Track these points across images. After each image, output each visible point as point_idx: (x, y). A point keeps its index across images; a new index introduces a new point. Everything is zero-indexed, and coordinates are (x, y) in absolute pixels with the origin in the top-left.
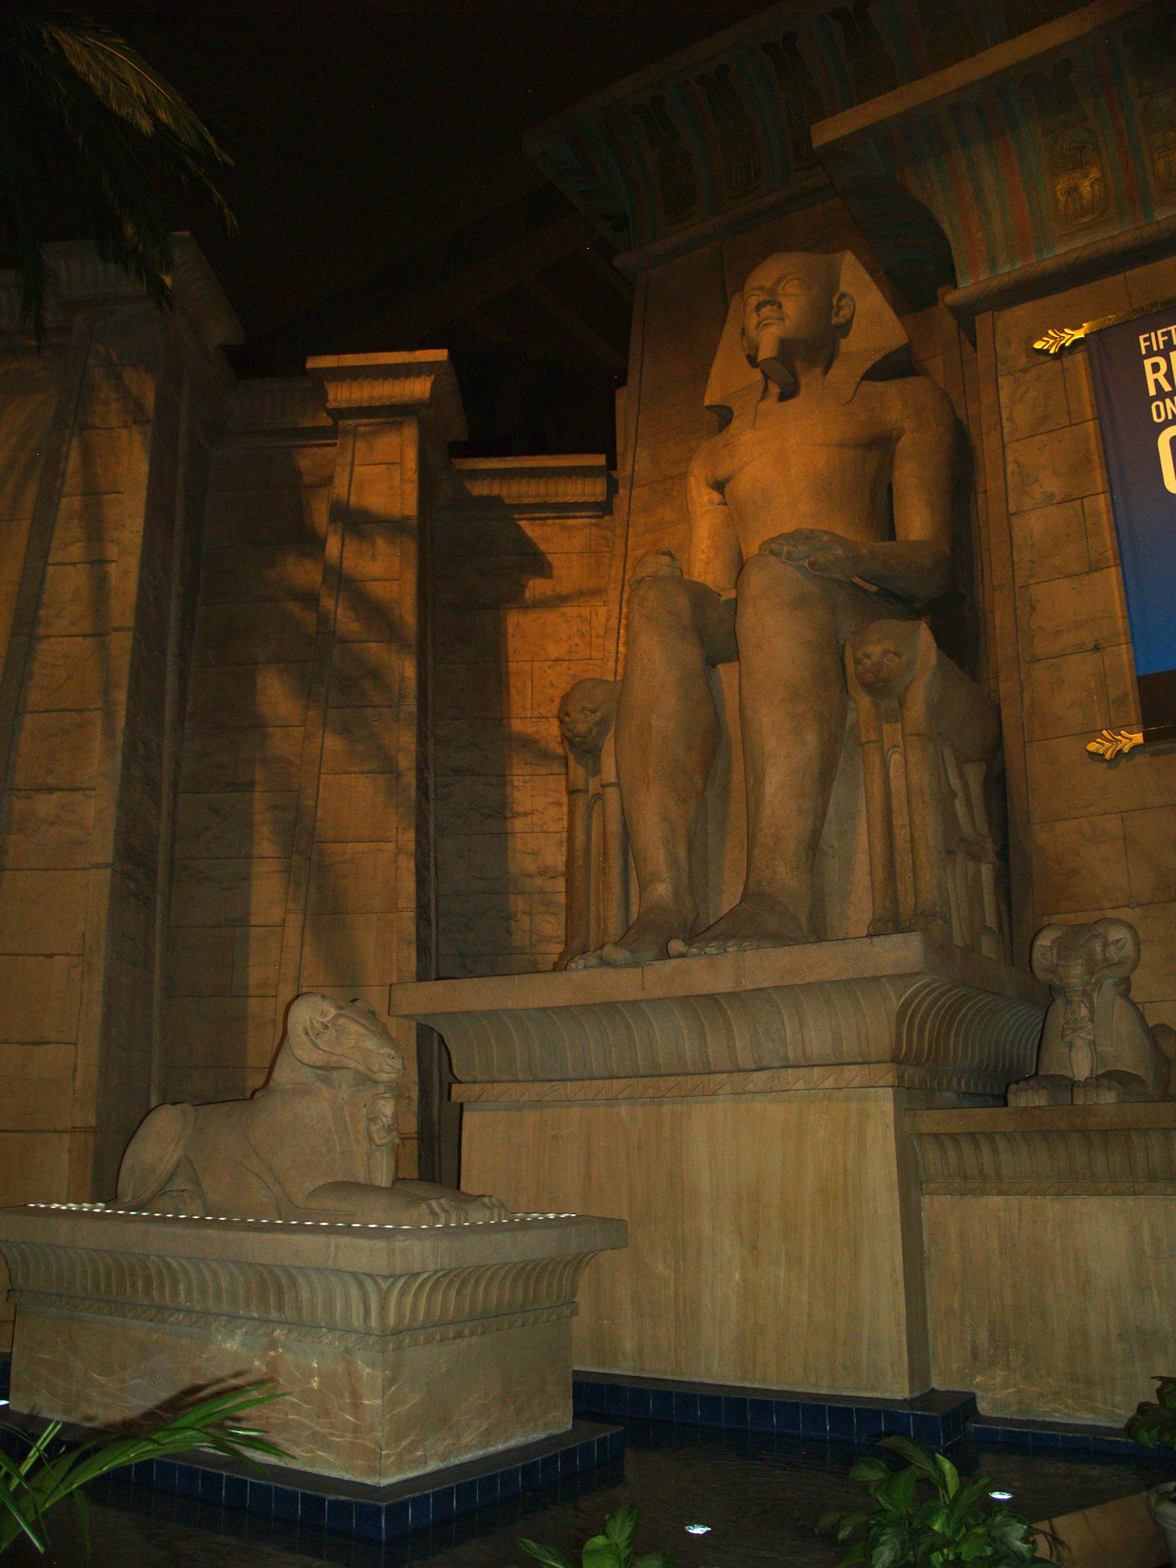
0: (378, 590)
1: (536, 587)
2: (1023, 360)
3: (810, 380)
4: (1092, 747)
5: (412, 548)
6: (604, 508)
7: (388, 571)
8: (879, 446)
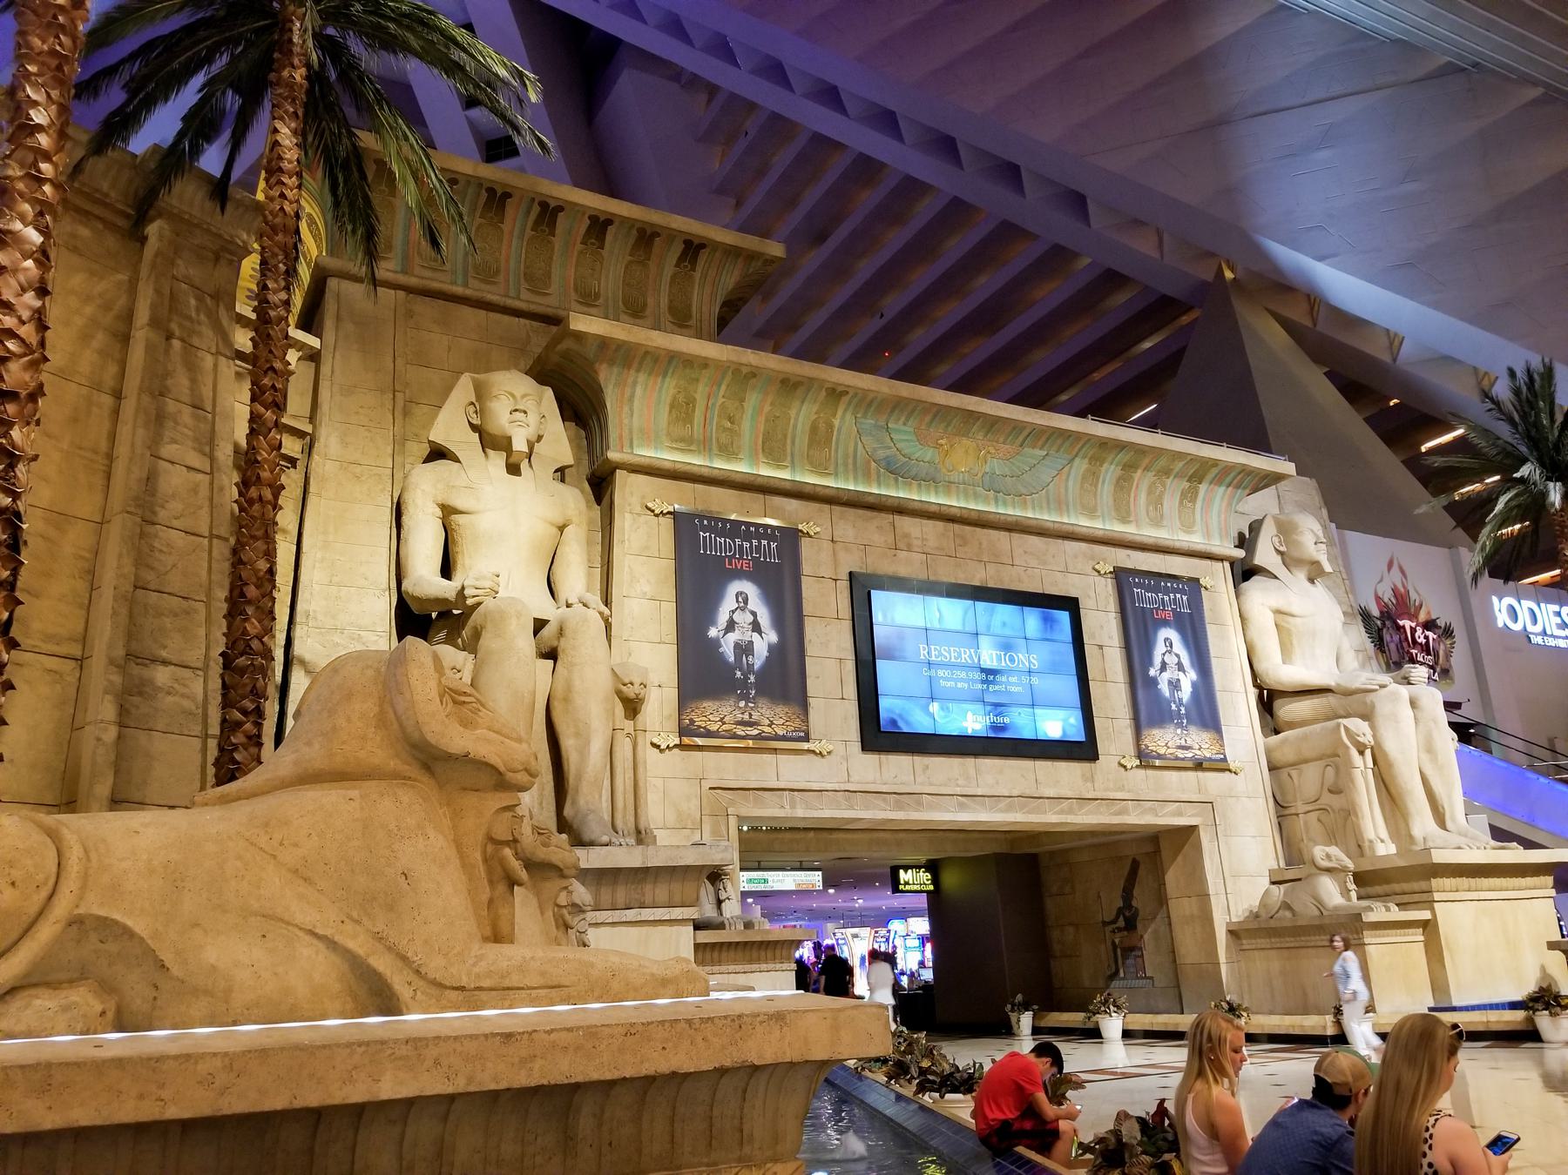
2: (638, 509)
3: (524, 465)
4: (655, 741)
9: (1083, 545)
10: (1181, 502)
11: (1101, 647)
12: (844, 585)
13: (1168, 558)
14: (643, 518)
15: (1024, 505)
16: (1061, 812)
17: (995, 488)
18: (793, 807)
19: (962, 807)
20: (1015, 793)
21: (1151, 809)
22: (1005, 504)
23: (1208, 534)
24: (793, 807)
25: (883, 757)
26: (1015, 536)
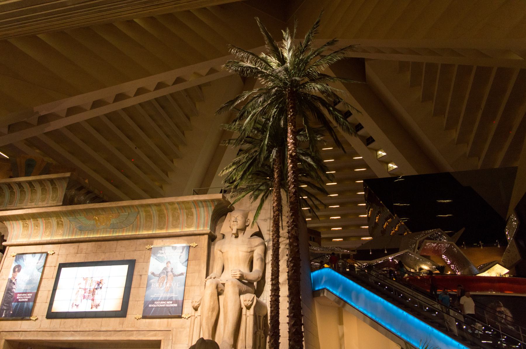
9: (144, 240)
10: (187, 217)
11: (141, 275)
15: (123, 232)
16: (107, 336)
17: (114, 228)
19: (72, 335)
20: (91, 330)
22: (116, 232)
23: (198, 226)
24: (25, 336)
25: (52, 320)
26: (119, 242)
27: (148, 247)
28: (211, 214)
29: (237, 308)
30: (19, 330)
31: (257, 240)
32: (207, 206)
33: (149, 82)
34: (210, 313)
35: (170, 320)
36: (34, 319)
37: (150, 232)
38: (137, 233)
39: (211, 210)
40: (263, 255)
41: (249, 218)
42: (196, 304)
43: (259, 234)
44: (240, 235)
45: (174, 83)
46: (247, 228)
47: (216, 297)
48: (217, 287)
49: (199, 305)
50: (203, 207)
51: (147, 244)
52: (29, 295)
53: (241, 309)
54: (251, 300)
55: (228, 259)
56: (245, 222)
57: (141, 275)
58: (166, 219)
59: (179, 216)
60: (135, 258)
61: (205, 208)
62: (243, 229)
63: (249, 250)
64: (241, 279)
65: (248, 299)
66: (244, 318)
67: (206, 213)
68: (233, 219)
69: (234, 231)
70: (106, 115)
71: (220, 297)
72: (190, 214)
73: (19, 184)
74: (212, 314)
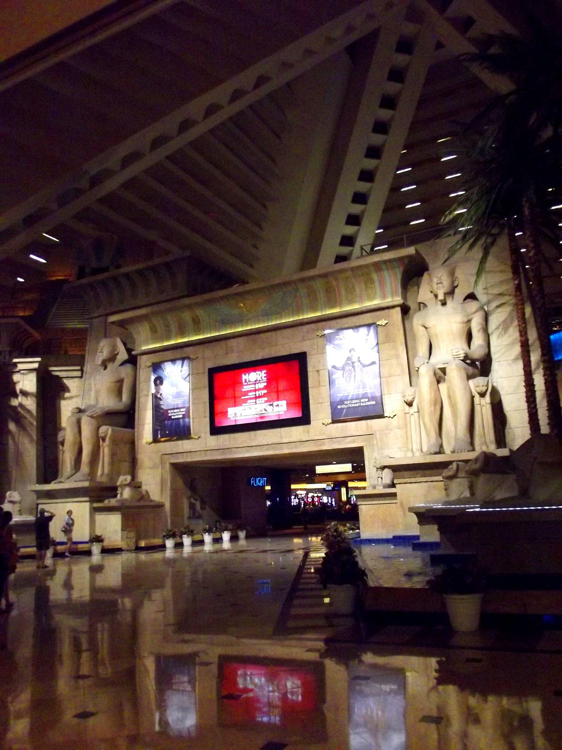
0: (29, 407)
1: (67, 395)
3: (110, 366)
5: (34, 399)
6: (81, 377)
7: (30, 404)
8: (120, 382)
9: (313, 326)
12: (207, 374)
13: (361, 316)
14: (145, 370)
17: (267, 315)
18: (187, 457)
19: (248, 451)
21: (337, 441)
27: (320, 333)
28: (399, 277)
29: (469, 397)
30: (183, 451)
31: (473, 306)
32: (392, 268)
33: (219, 94)
34: (433, 408)
35: (369, 421)
36: (196, 437)
37: (318, 314)
38: (301, 318)
39: (398, 273)
40: (484, 323)
41: (456, 275)
42: (409, 399)
43: (472, 297)
44: (449, 302)
45: (257, 86)
46: (457, 290)
47: (436, 387)
48: (435, 374)
49: (414, 398)
50: (388, 269)
51: (318, 330)
52: (182, 410)
53: (473, 397)
54: (485, 384)
55: (436, 336)
56: (453, 282)
57: (318, 371)
58: (337, 293)
59: (353, 287)
60: (305, 351)
61: (390, 271)
62: (451, 293)
63: (466, 320)
64: (466, 359)
65: (481, 384)
66: (477, 408)
67: (392, 278)
68: (435, 280)
69: (441, 297)
70: (168, 158)
71: (440, 385)
72: (369, 281)
73: (127, 276)
74: (435, 408)
